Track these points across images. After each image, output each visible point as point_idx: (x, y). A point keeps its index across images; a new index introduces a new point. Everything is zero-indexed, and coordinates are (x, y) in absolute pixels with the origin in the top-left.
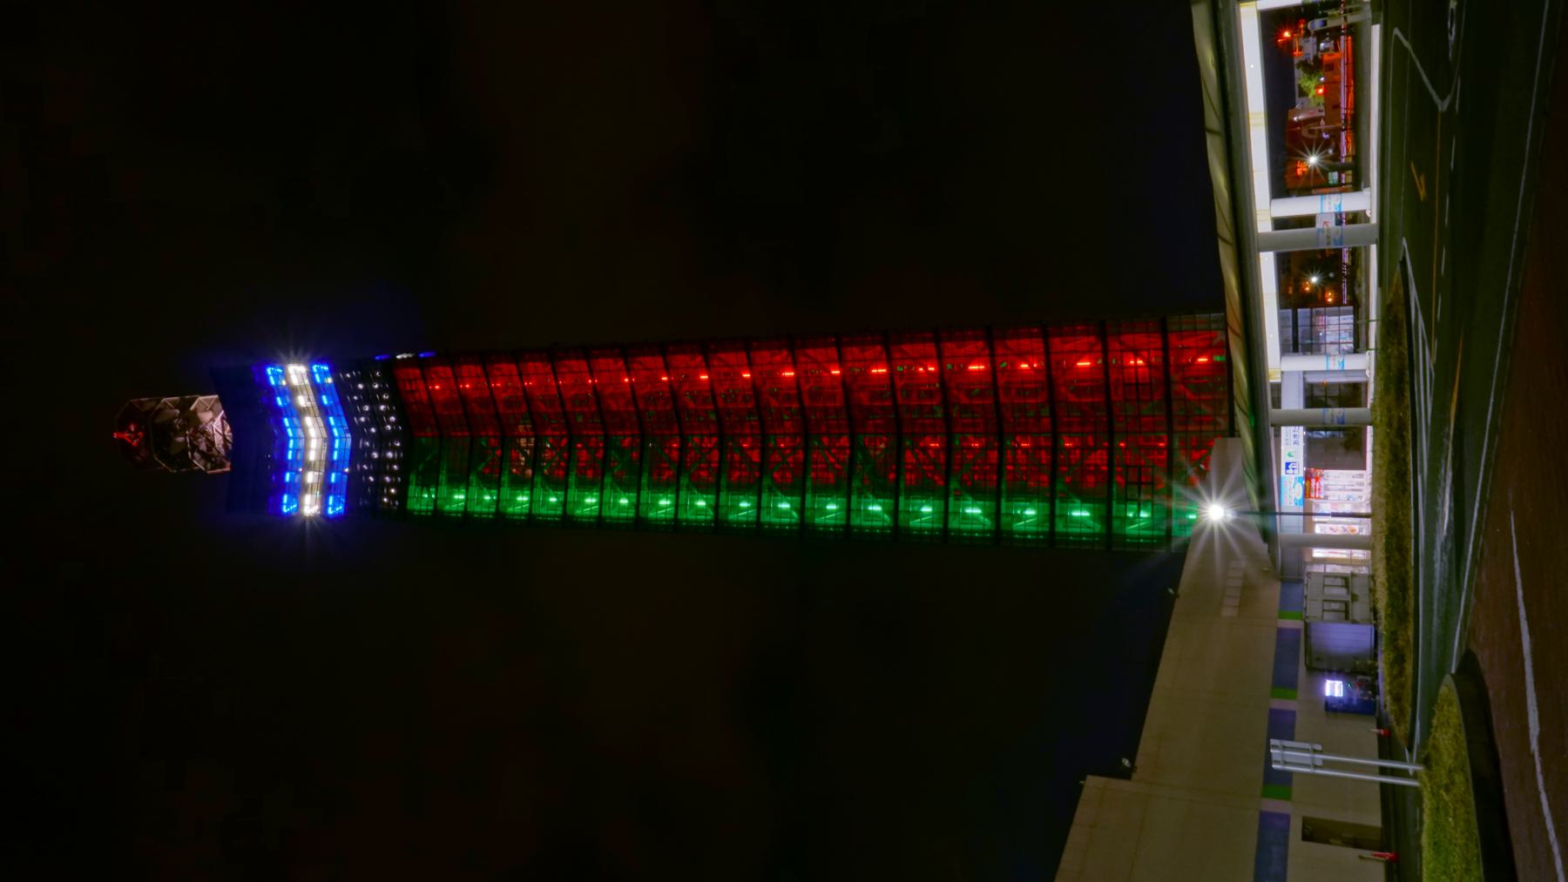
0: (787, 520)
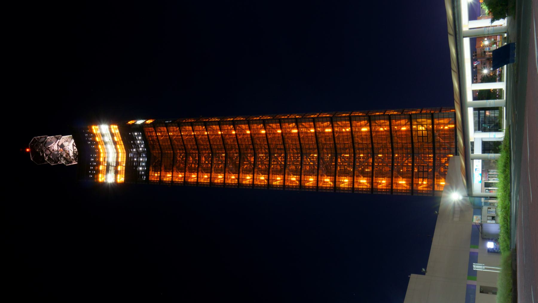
0: (295, 184)
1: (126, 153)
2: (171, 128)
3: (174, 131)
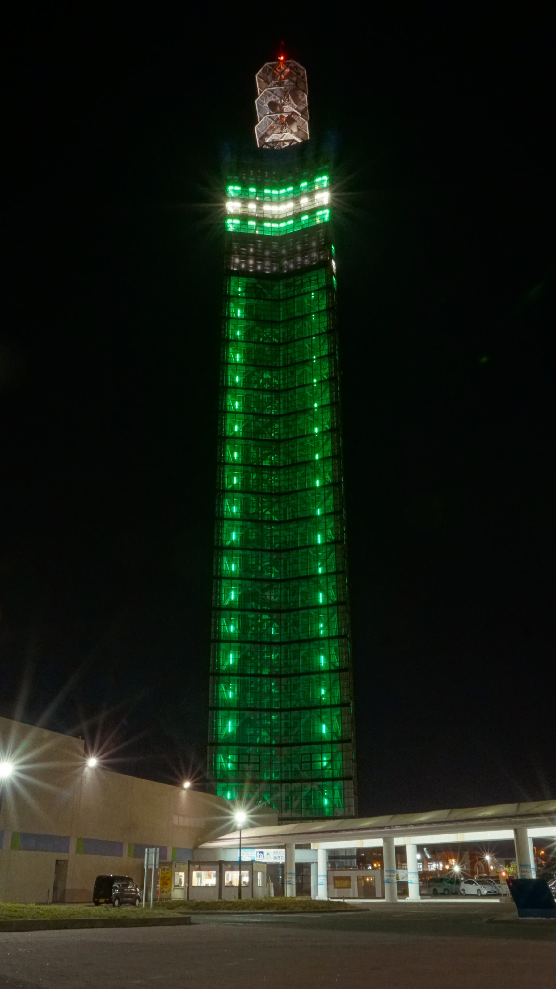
0: (225, 539)
1: (279, 236)
2: (324, 319)
3: (319, 323)
